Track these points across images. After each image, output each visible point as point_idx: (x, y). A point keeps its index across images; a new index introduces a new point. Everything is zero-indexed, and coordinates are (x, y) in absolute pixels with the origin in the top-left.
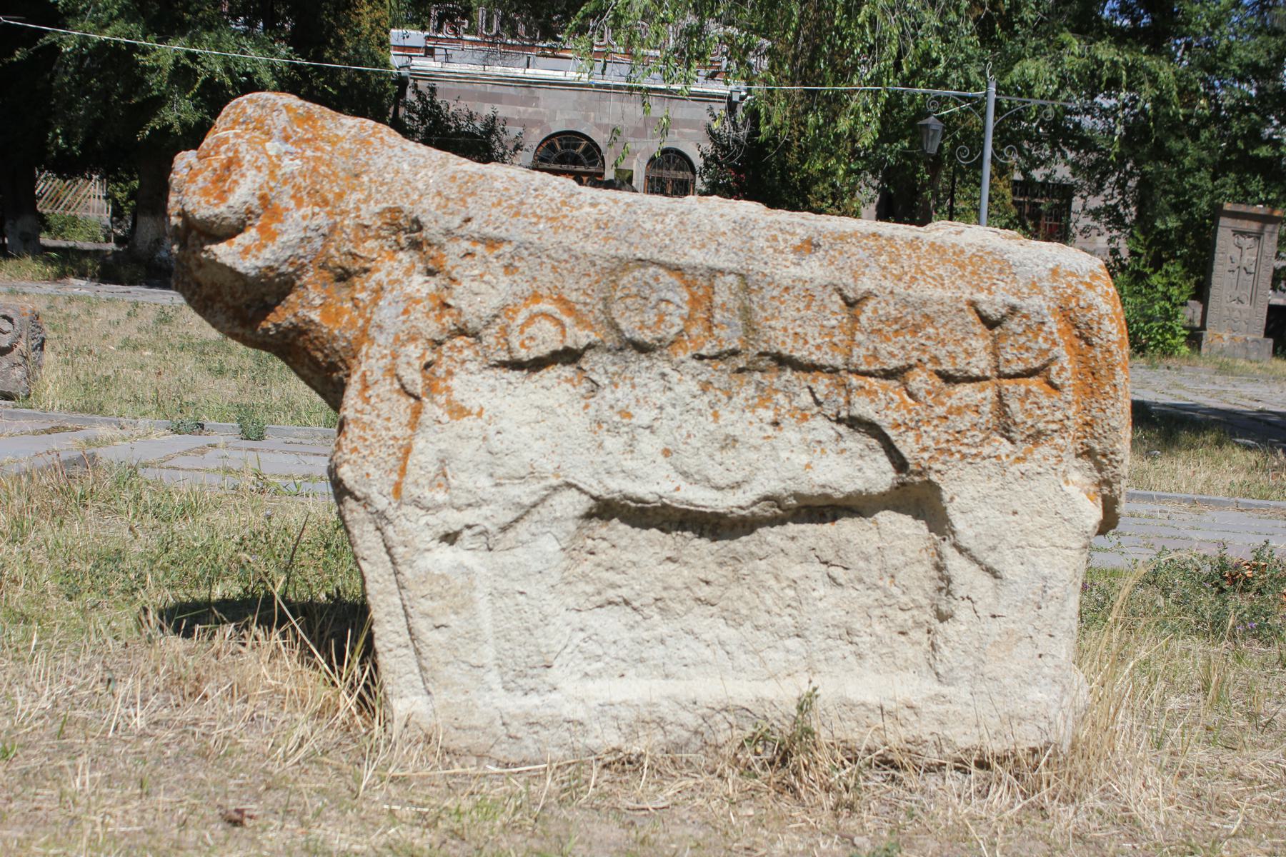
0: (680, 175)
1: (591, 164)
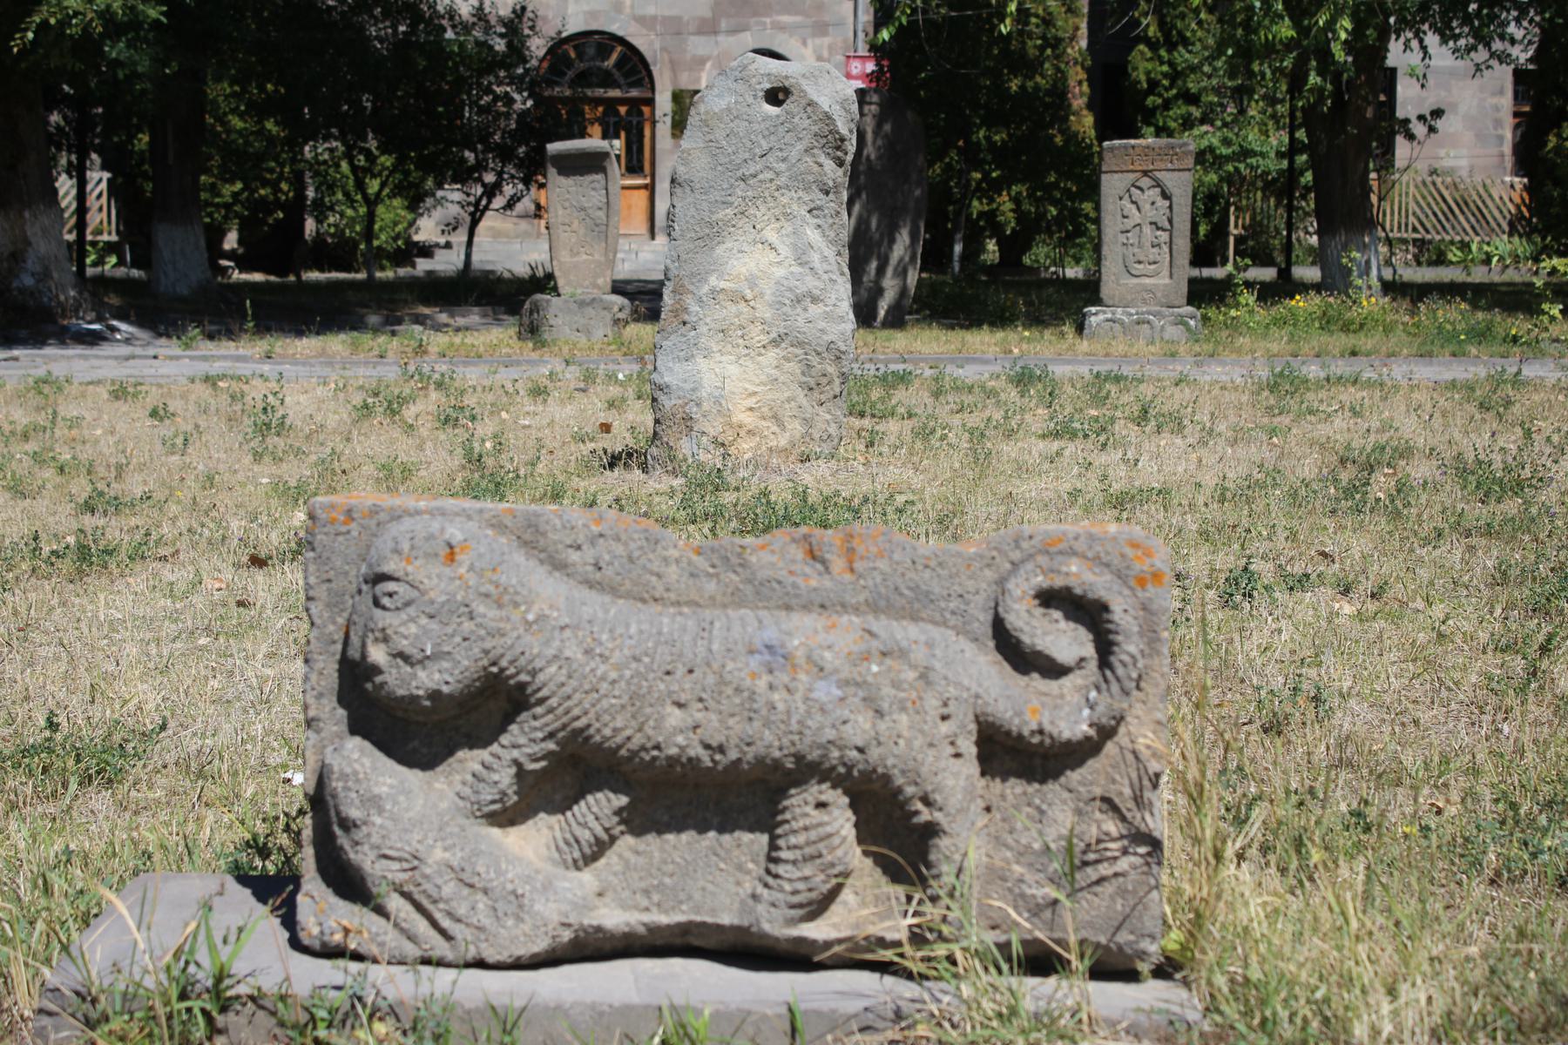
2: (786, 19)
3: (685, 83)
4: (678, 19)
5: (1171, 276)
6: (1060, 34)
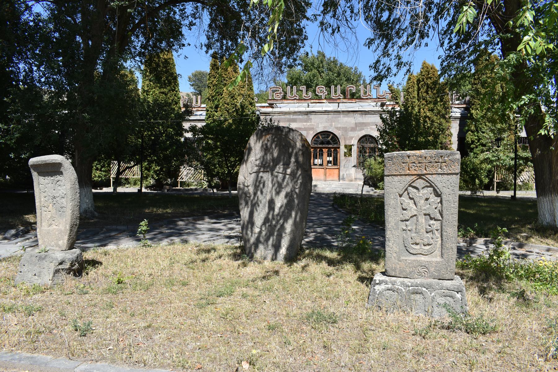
0: (372, 145)
1: (334, 144)
3: (348, 143)
5: (442, 255)
6: (444, 127)
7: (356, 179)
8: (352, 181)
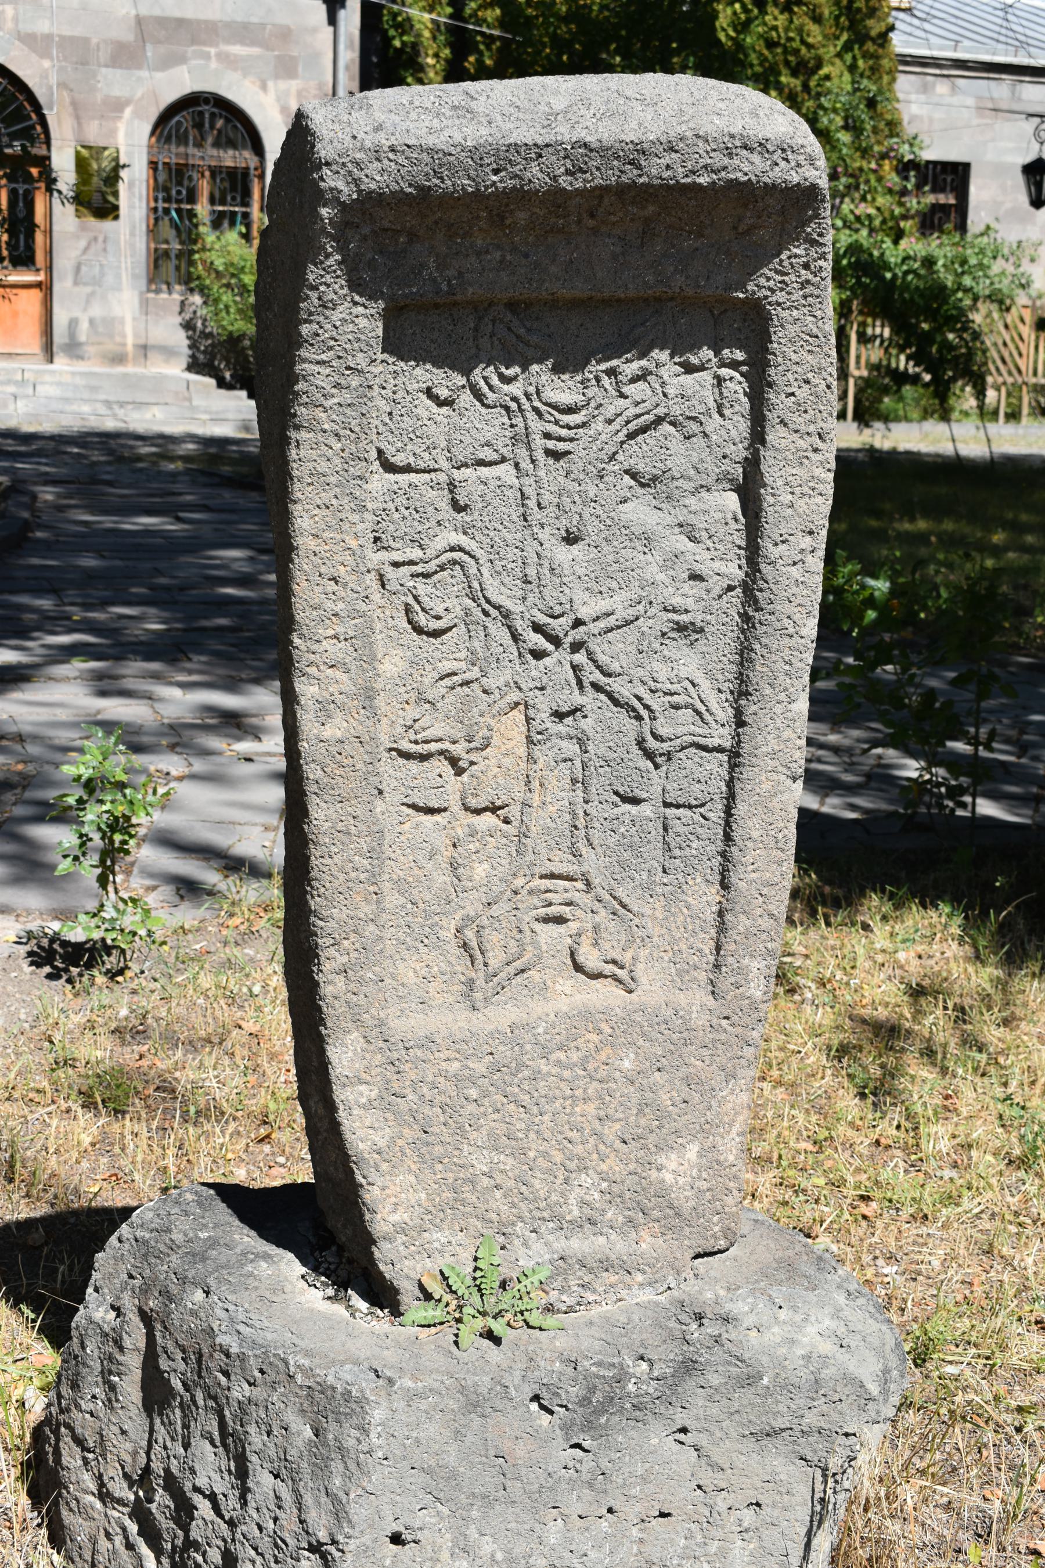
0: (229, 158)
2: (237, 50)
3: (94, 135)
4: (86, 41)
7: (144, 349)
8: (119, 359)
